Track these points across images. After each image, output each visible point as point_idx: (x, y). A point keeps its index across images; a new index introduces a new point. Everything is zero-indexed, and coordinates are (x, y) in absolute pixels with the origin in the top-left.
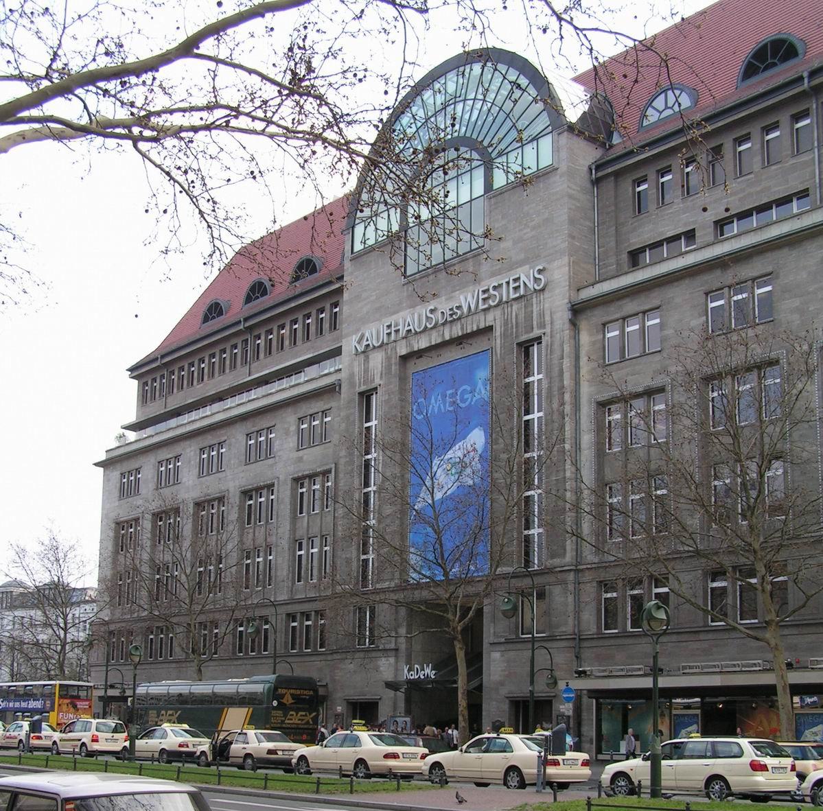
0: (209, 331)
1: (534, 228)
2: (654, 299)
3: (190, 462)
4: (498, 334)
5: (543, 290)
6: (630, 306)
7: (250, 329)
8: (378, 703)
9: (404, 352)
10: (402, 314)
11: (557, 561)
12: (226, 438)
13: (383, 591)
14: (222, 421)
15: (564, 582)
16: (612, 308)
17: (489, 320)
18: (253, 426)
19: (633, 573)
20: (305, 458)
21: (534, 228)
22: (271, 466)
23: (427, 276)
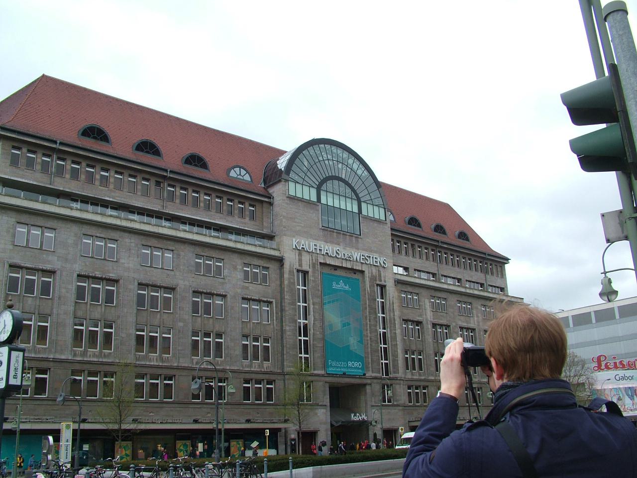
0: (133, 158)
1: (379, 241)
2: (416, 290)
3: (130, 249)
4: (368, 276)
5: (385, 268)
6: (410, 289)
7: (170, 178)
8: (317, 432)
9: (322, 261)
10: (320, 242)
11: (397, 375)
12: (174, 248)
13: (318, 375)
14: (110, 224)
15: (400, 384)
16: (404, 286)
17: (364, 268)
18: (203, 252)
19: (418, 384)
20: (250, 288)
21: (379, 241)
22: (223, 284)
23: (333, 232)
